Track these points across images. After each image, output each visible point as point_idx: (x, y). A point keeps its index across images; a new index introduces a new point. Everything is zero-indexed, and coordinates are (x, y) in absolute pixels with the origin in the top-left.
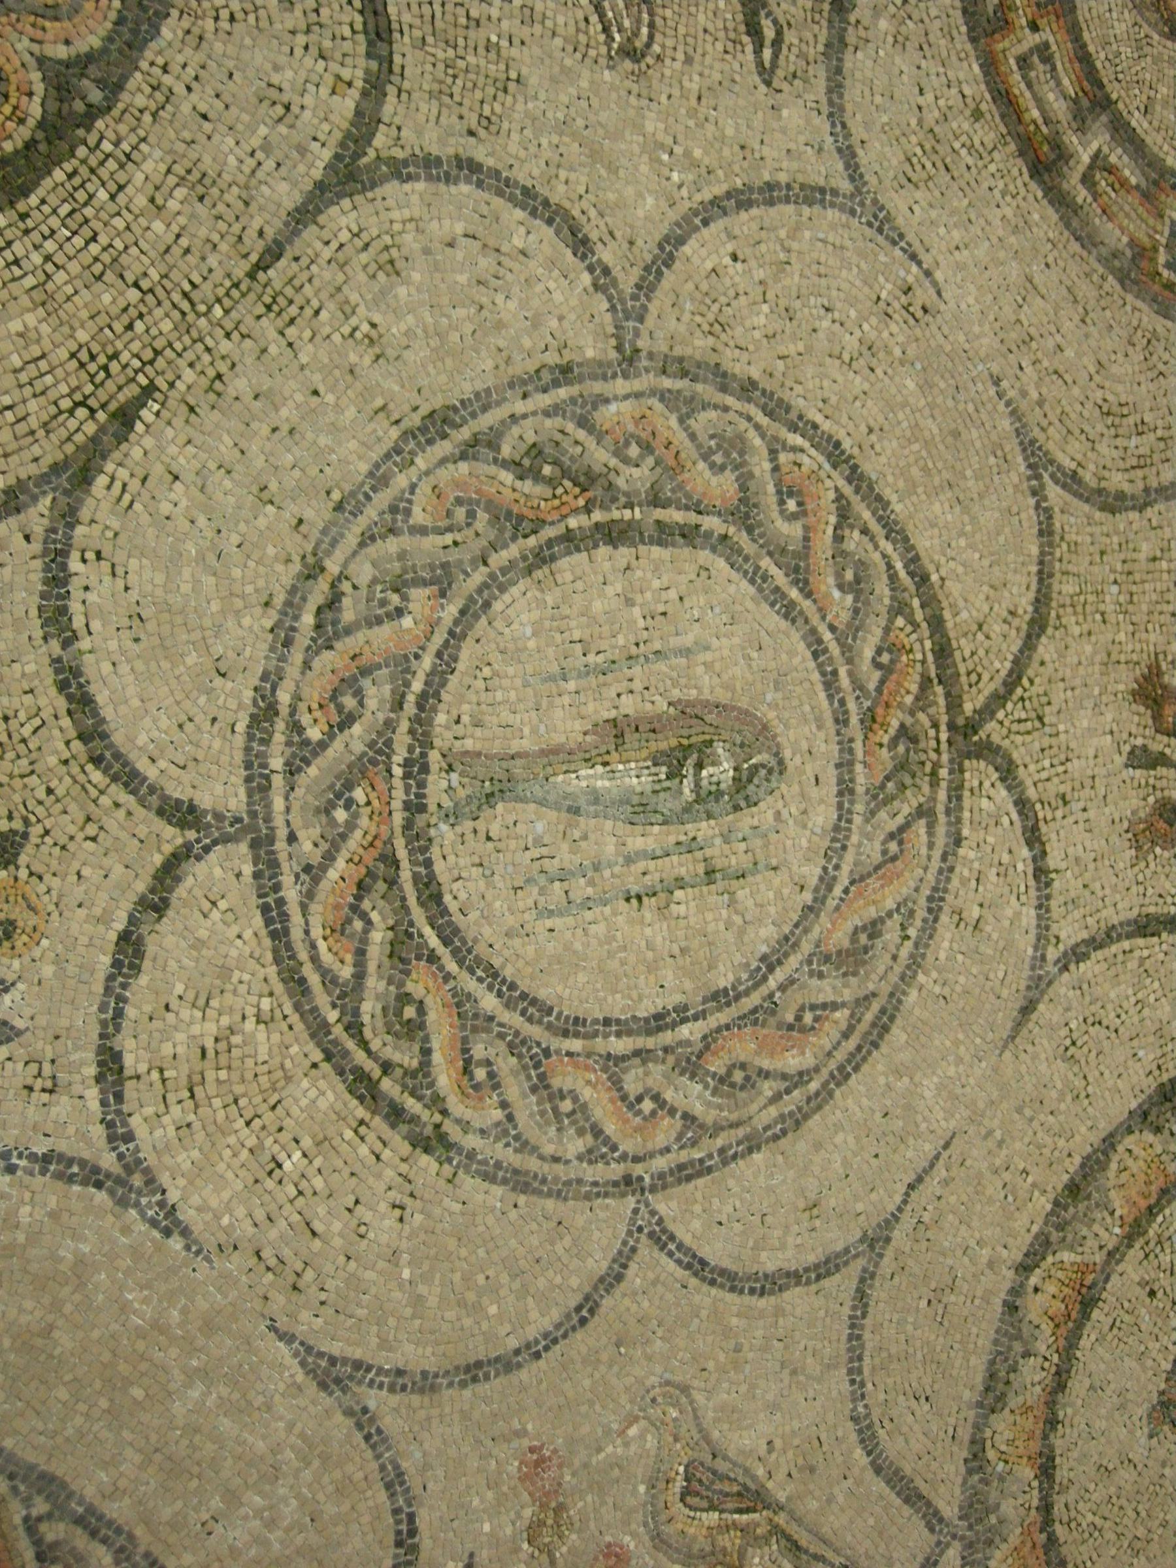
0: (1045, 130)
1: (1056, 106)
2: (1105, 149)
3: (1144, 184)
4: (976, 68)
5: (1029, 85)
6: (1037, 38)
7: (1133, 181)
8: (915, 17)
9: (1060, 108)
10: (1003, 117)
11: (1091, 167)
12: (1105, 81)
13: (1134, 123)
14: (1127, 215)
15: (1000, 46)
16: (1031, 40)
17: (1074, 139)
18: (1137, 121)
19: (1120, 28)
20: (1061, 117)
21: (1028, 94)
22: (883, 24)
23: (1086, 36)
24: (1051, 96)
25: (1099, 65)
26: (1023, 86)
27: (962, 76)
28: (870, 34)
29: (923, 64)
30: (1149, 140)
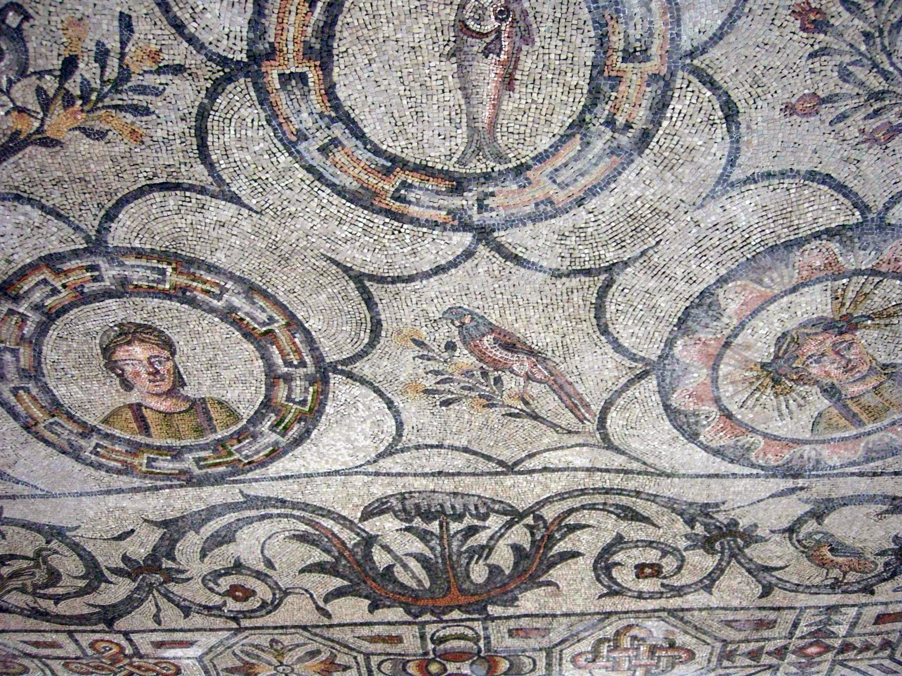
0: (21, 292)
1: (35, 297)
2: (31, 319)
3: (27, 336)
4: (28, 261)
5: (37, 285)
6: (60, 288)
7: (25, 332)
8: (34, 232)
9: (37, 297)
10: (15, 273)
11: (19, 313)
12: (61, 319)
13: (51, 332)
14: (8, 330)
15: (45, 270)
16: (58, 285)
17: (26, 306)
18: (52, 334)
19: (89, 325)
20: (32, 300)
21: (32, 284)
22: (22, 218)
23: (76, 310)
24: (38, 295)
25: (66, 316)
26: (34, 282)
27: (21, 254)
28: (14, 212)
29: (15, 237)
30: (47, 338)
